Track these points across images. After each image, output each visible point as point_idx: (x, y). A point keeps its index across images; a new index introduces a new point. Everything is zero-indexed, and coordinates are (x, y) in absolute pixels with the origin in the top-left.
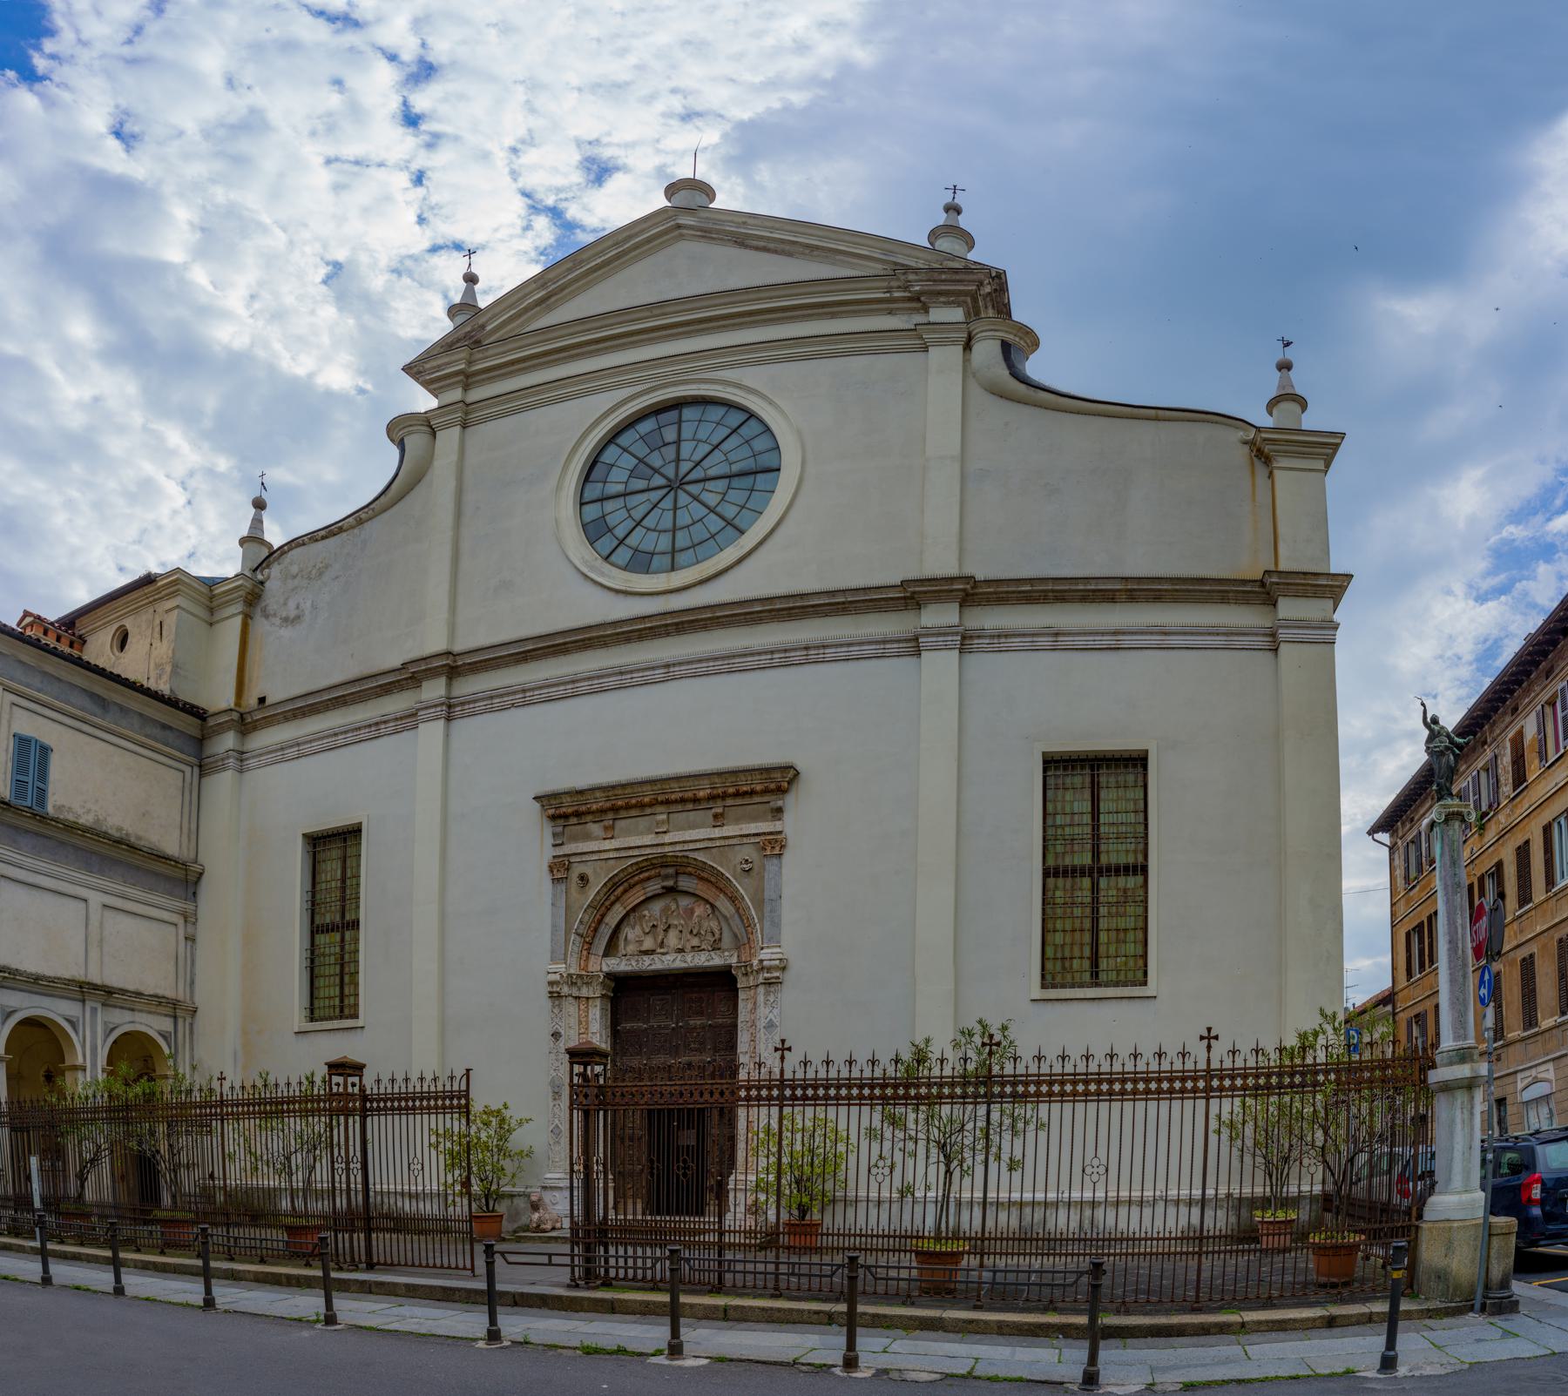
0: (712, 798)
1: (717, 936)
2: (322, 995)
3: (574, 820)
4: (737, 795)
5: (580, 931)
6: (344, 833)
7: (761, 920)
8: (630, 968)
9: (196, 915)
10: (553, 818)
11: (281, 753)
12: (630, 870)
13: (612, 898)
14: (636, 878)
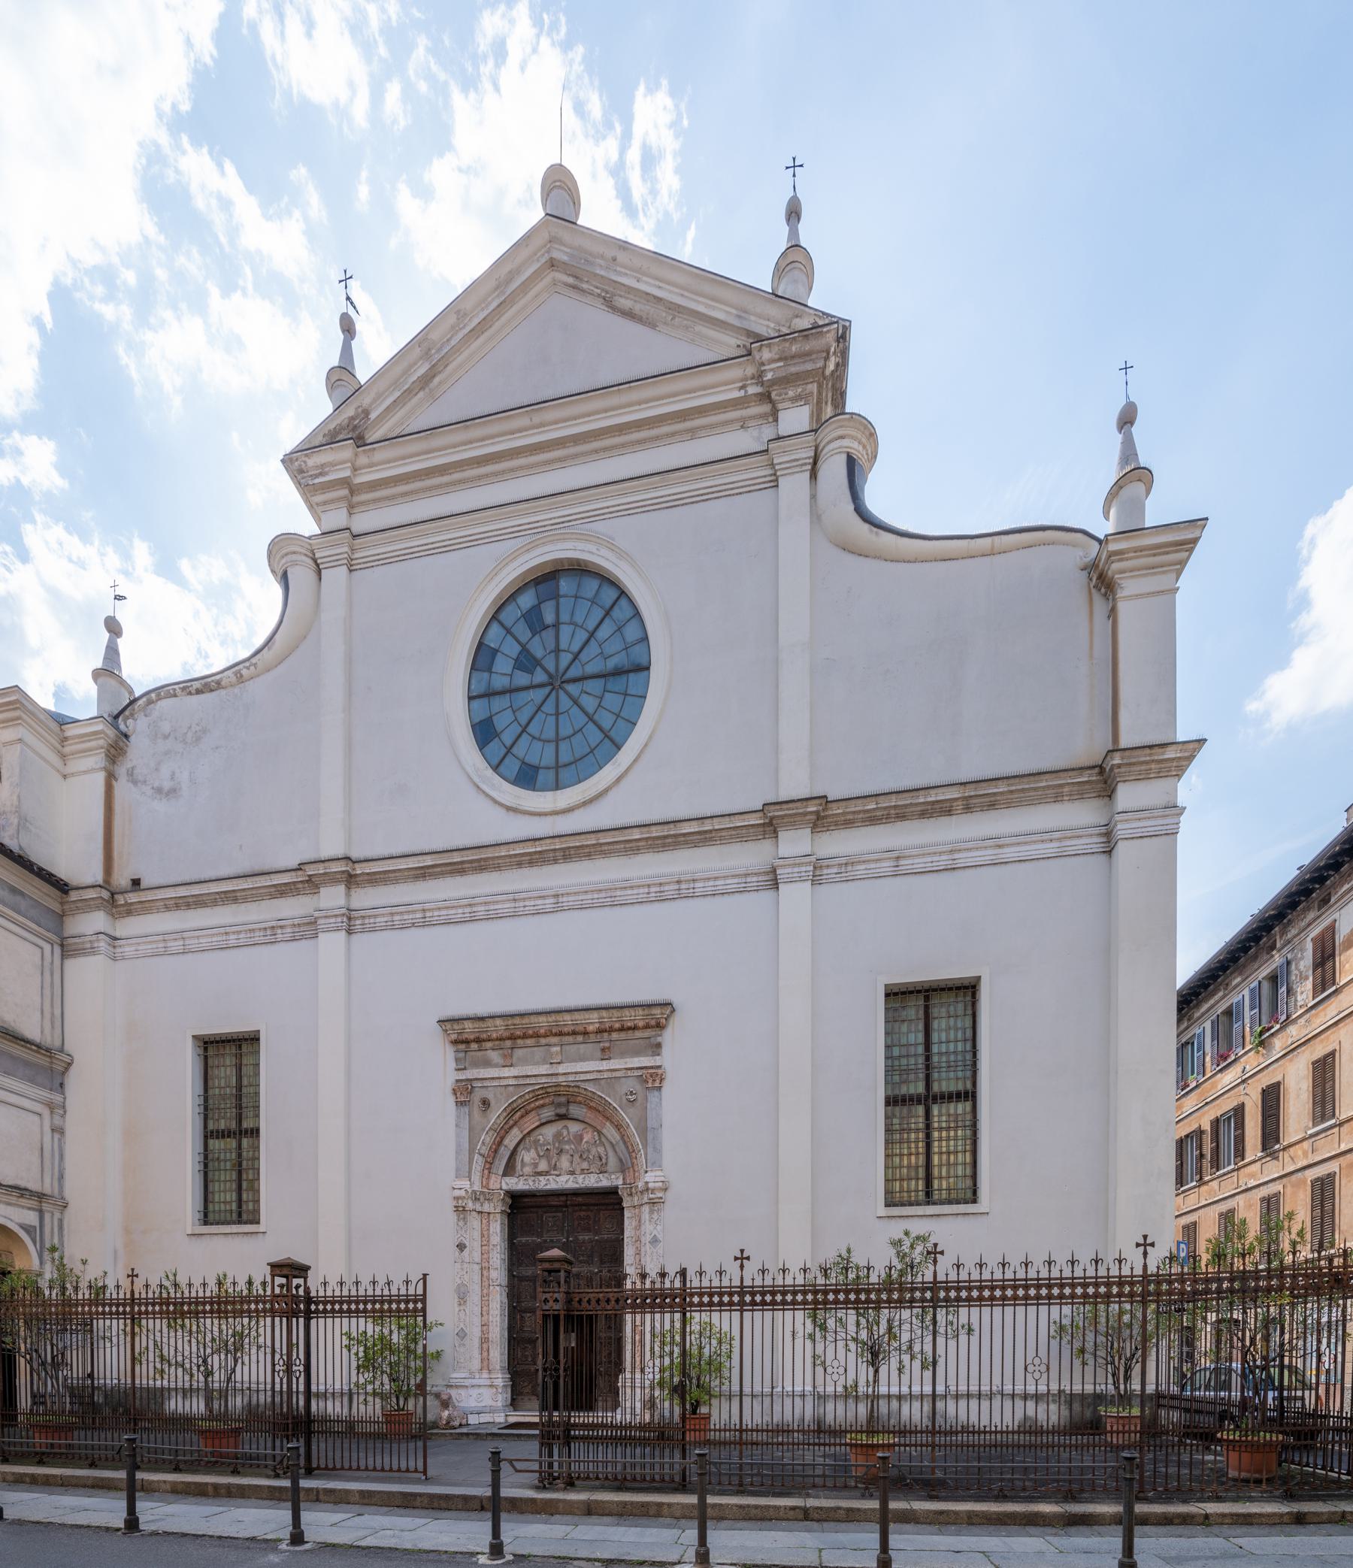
0: (600, 1031)
2: (217, 1200)
3: (474, 1046)
4: (622, 1029)
5: (482, 1152)
6: (239, 1040)
7: (645, 1146)
8: (527, 1187)
9: (64, 1107)
10: (455, 1042)
11: (164, 947)
12: (527, 1097)
13: (511, 1122)
14: (533, 1105)
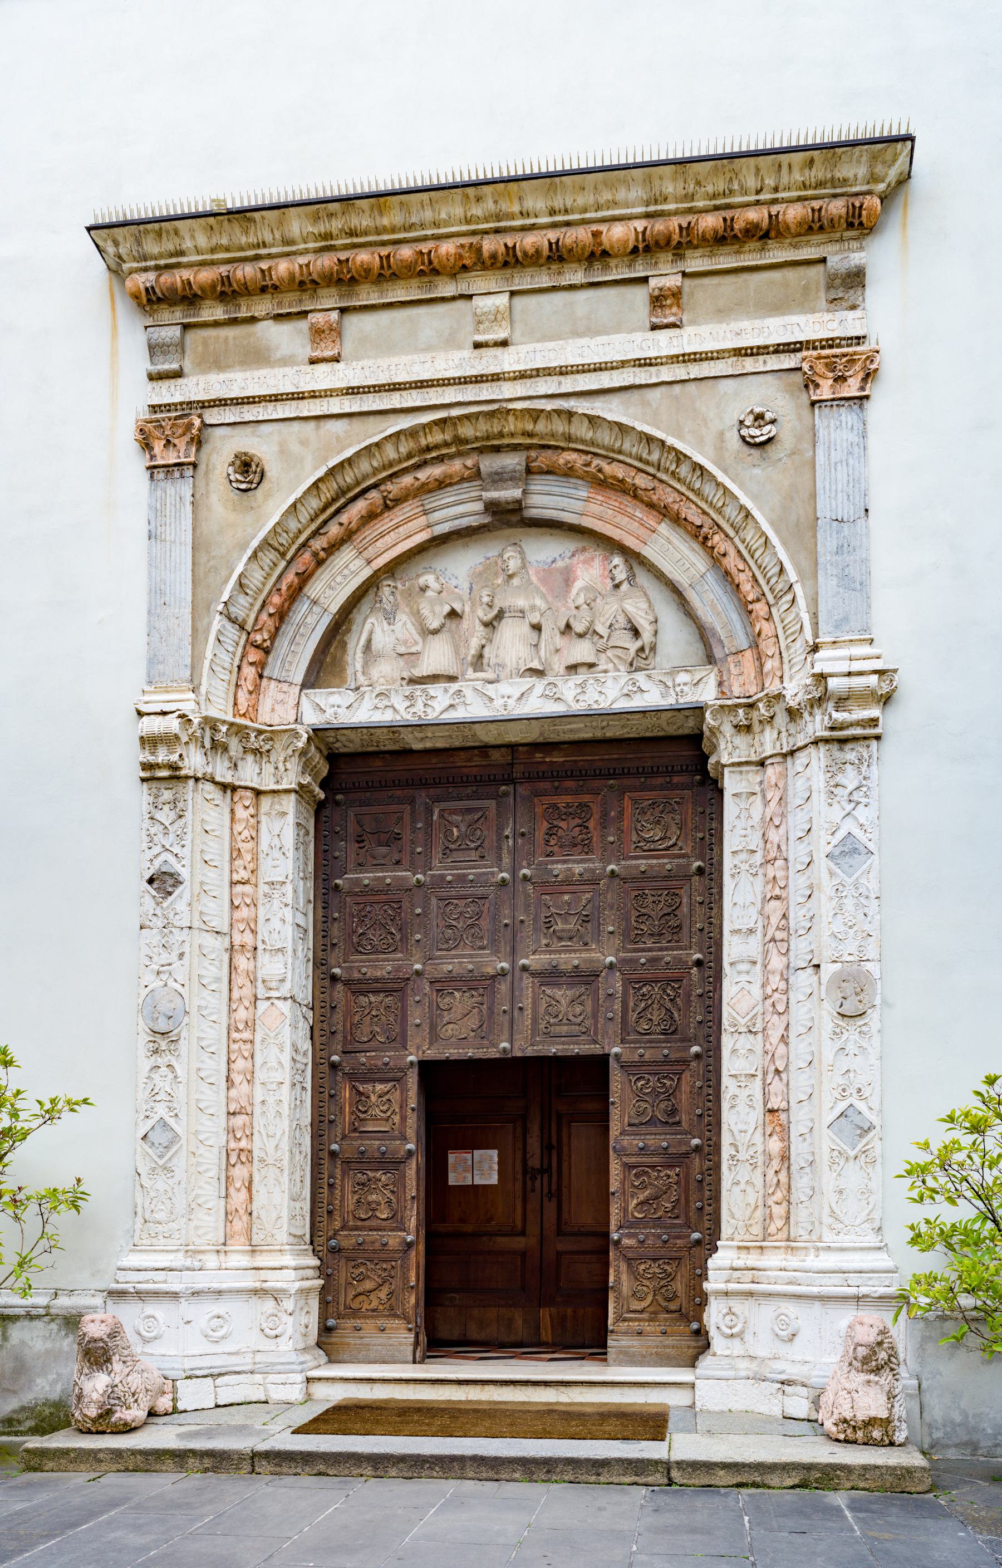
1: (647, 637)
13: (334, 530)
14: (407, 480)
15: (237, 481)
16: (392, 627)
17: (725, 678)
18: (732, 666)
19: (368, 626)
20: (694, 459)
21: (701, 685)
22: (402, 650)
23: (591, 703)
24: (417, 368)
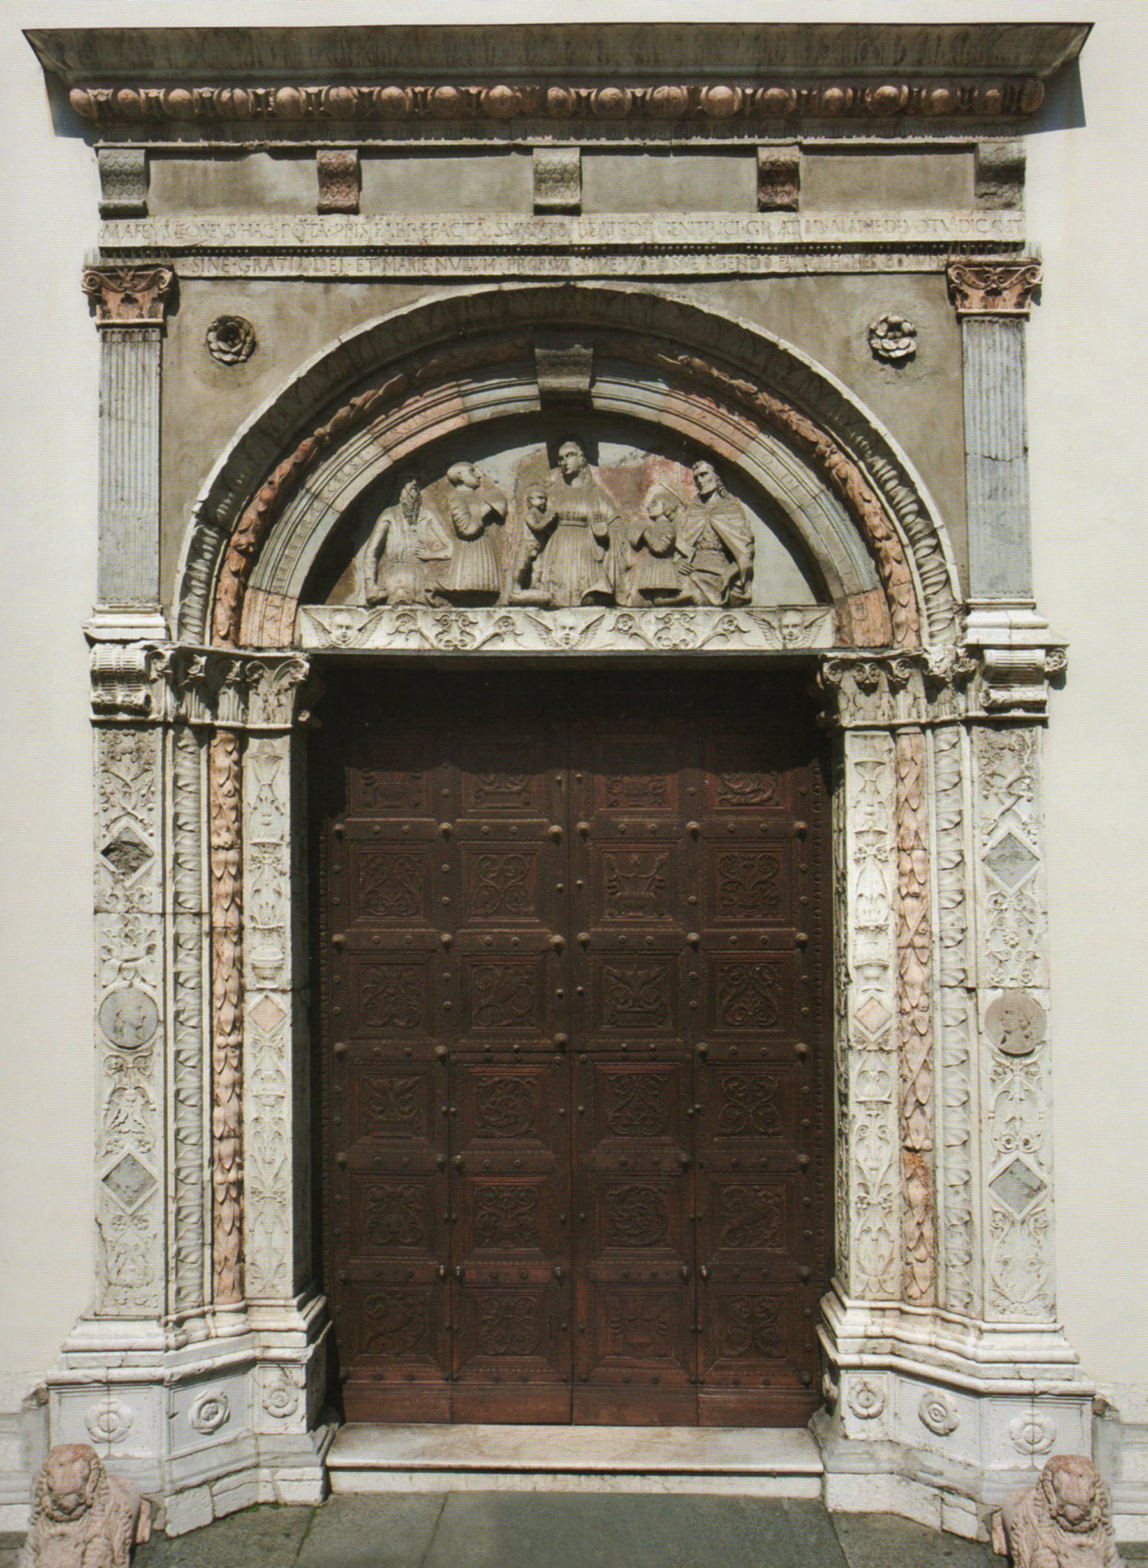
1: (743, 562)
15: (221, 350)
16: (413, 527)
17: (845, 622)
18: (853, 609)
19: (380, 526)
20: (814, 369)
21: (814, 629)
22: (427, 554)
23: (677, 642)
24: (458, 230)
